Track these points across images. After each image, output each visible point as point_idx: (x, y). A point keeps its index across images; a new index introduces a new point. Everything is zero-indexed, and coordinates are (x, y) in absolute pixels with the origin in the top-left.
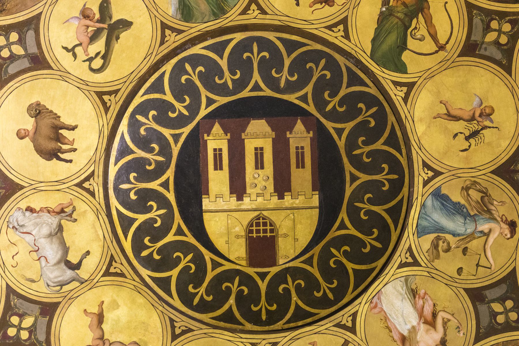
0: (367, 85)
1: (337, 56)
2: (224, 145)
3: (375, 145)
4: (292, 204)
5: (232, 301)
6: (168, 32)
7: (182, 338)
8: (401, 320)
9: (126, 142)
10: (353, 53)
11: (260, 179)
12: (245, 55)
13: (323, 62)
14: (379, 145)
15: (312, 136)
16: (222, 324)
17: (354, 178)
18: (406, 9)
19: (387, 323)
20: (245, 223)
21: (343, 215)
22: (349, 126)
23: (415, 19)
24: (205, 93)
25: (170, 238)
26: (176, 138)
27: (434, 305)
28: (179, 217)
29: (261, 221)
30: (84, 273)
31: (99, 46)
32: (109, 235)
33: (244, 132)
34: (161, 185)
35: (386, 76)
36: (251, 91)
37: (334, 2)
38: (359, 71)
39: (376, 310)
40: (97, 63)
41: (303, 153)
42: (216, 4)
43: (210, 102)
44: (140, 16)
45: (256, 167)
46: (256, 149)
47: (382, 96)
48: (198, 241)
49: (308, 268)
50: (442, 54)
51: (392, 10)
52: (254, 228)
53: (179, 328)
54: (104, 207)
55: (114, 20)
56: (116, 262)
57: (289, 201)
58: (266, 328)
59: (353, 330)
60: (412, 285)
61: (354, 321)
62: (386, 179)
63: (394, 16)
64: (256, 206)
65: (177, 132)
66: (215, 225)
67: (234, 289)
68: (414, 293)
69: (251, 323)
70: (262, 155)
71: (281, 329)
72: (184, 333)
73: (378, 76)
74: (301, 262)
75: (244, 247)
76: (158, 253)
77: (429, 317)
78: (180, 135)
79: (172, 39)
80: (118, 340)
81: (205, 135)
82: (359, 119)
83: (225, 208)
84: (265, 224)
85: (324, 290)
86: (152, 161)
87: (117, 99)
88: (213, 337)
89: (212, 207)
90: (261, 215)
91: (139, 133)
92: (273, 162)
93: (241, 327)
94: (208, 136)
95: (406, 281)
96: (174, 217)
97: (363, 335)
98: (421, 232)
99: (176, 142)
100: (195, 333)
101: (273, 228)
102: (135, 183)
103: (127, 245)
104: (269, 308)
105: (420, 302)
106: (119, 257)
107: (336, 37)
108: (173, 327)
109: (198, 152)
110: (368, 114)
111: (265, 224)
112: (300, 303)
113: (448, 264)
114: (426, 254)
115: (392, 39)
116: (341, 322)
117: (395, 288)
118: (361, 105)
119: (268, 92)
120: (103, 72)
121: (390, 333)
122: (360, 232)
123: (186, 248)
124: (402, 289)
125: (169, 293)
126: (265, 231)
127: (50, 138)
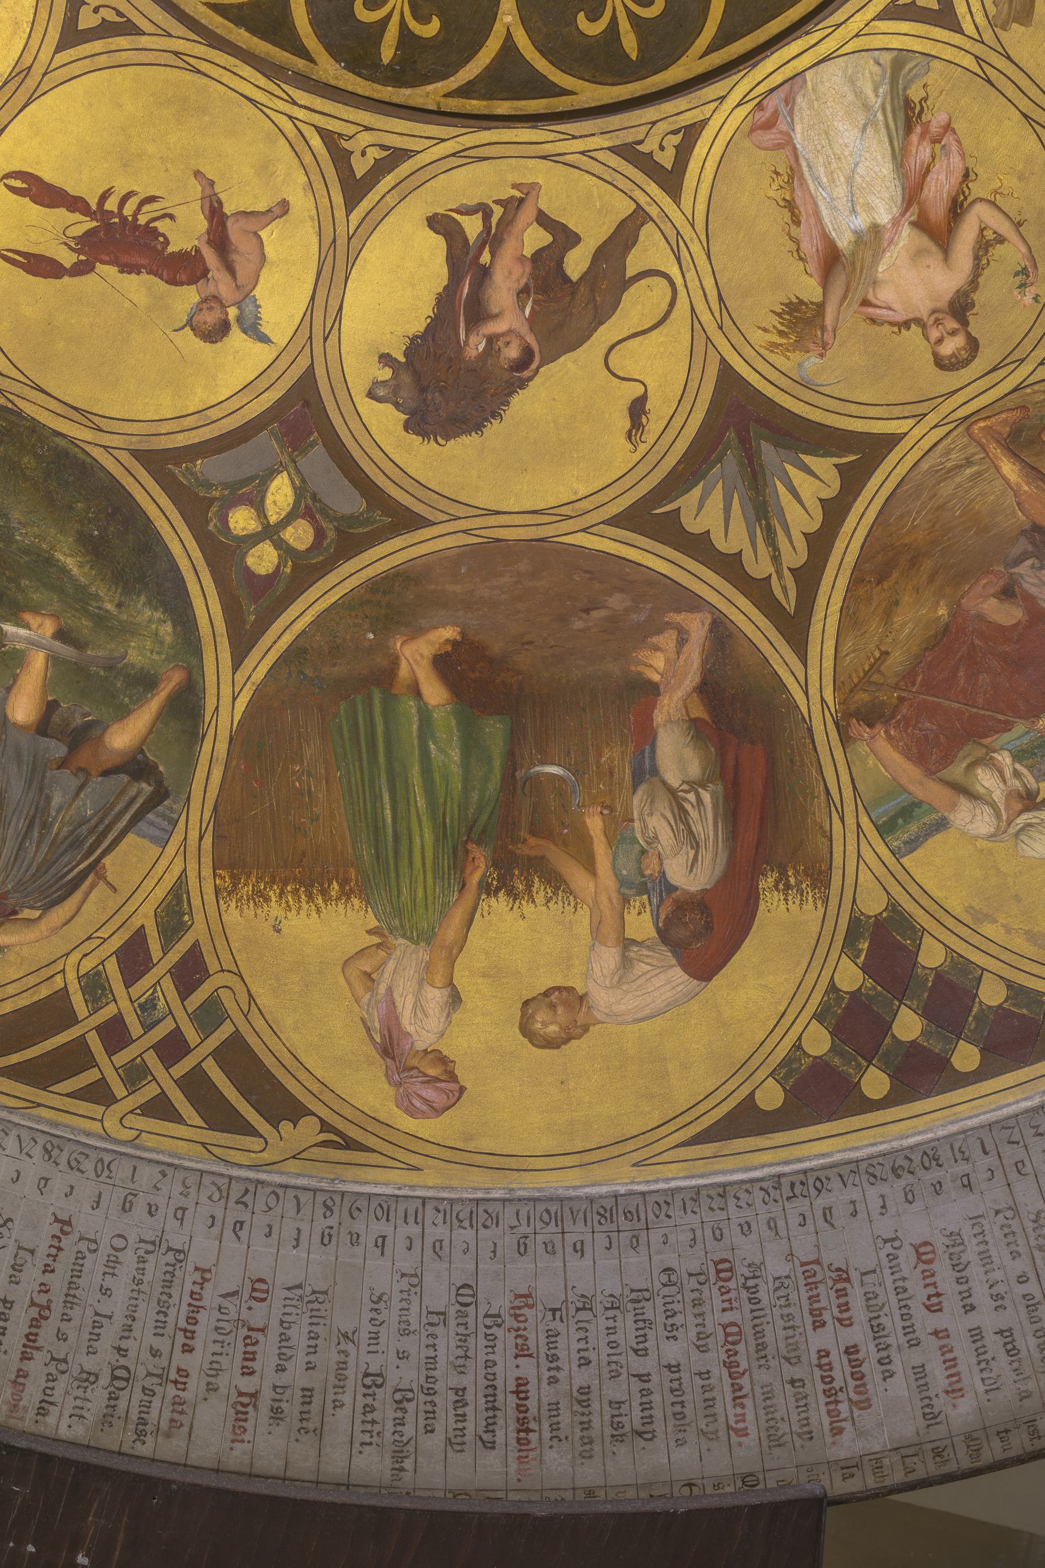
7: (97, 46)
8: (841, 191)
16: (241, 36)
19: (793, 191)
27: (966, 175)
39: (769, 137)
59: (672, 181)
60: (913, 87)
68: (908, 116)
71: (433, 107)
77: (938, 211)
85: (614, 18)
88: (199, 72)
93: (300, 64)
95: (897, 65)
100: (144, 41)
104: (413, 24)
112: (522, 40)
116: (641, 142)
117: (852, 81)
121: (793, 227)
124: (876, 90)
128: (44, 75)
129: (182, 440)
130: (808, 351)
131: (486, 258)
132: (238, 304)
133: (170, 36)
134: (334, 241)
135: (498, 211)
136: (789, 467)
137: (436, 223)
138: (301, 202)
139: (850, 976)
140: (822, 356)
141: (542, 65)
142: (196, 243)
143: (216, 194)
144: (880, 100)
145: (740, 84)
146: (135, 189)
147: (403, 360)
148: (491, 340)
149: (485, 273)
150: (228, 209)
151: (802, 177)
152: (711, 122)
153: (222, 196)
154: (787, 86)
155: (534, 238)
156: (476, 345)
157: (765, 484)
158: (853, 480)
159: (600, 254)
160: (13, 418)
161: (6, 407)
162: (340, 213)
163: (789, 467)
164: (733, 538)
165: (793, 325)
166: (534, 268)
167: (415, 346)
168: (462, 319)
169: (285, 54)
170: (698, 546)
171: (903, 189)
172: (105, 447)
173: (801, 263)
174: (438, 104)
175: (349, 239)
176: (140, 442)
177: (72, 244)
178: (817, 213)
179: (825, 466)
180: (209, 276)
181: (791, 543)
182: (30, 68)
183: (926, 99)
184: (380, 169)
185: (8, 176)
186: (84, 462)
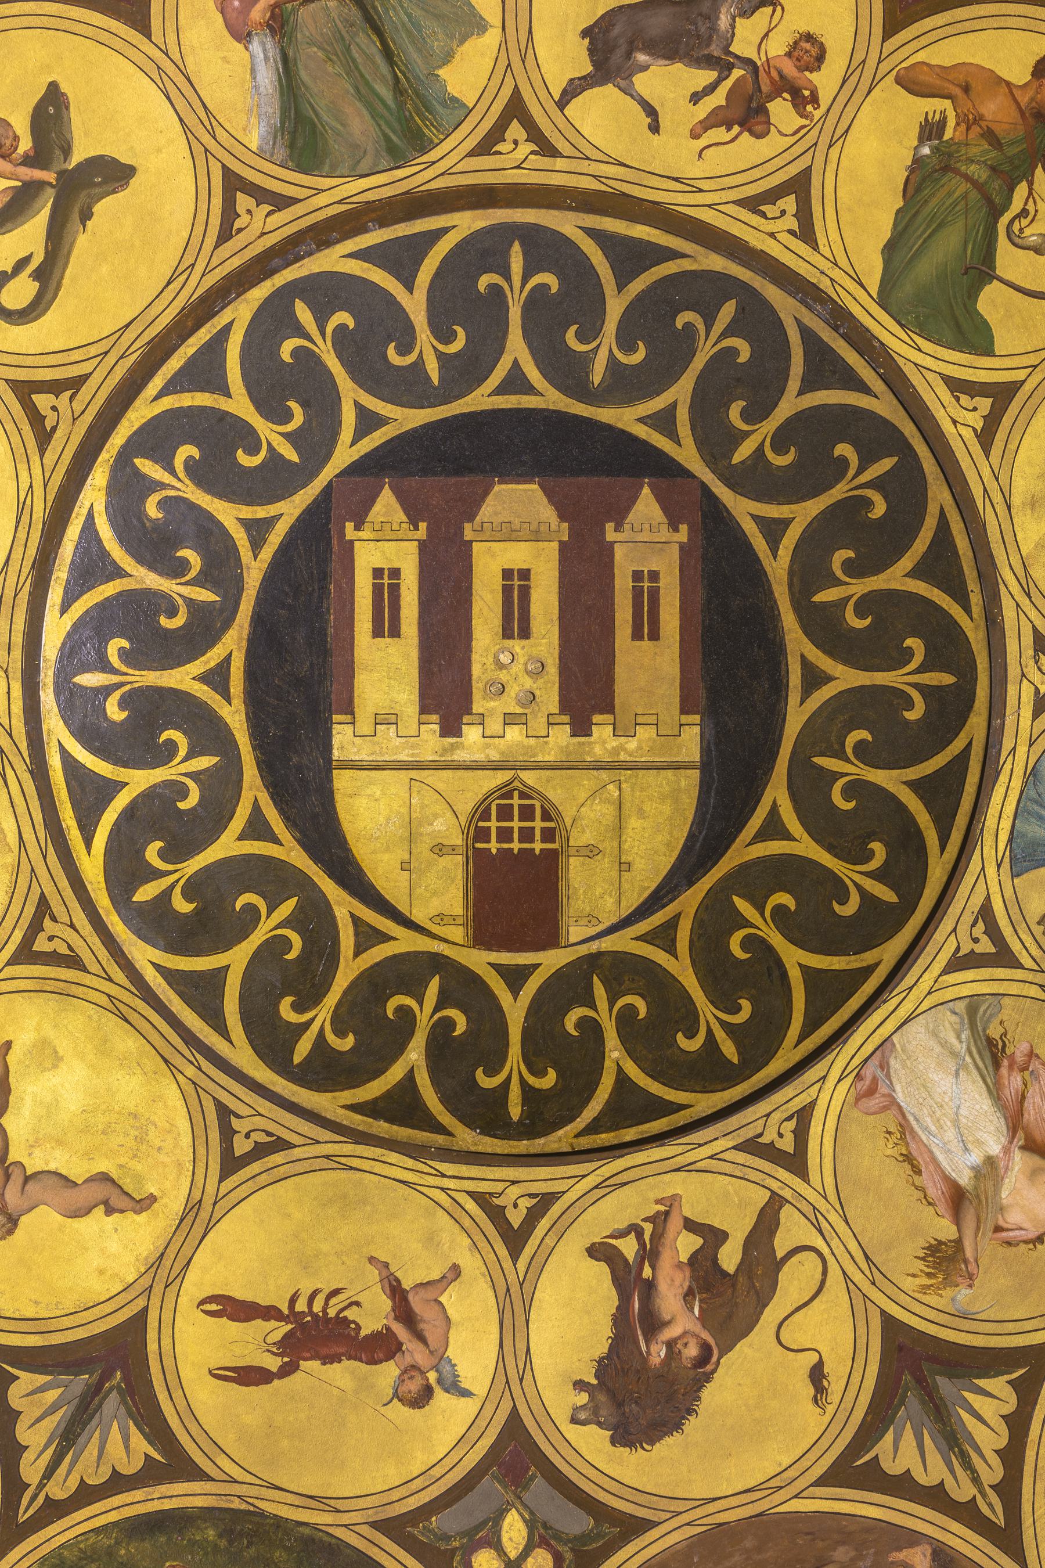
0: (863, 388)
1: (772, 293)
2: (405, 557)
3: (882, 576)
4: (616, 751)
5: (415, 1054)
6: (244, 202)
8: (951, 1134)
9: (99, 541)
10: (825, 284)
11: (517, 668)
12: (484, 282)
13: (728, 311)
14: (897, 577)
15: (686, 540)
16: (382, 1128)
17: (814, 679)
18: (994, 154)
19: (907, 1145)
20: (465, 806)
21: (777, 793)
22: (804, 513)
23: (1024, 184)
24: (352, 394)
25: (227, 845)
26: (257, 530)
28: (259, 781)
29: (516, 801)
31: (29, 237)
32: (36, 835)
33: (471, 518)
34: (204, 678)
35: (927, 362)
36: (499, 391)
37: (769, 123)
38: (842, 343)
39: (874, 1102)
40: (20, 292)
41: (654, 594)
42: (399, 121)
43: (368, 422)
44: (159, 150)
45: (504, 629)
46: (507, 574)
47: (912, 424)
48: (316, 858)
49: (661, 957)
51: (950, 155)
52: (493, 824)
53: (247, 1136)
54: (24, 746)
55: (77, 158)
56: (54, 919)
57: (604, 742)
58: (523, 1146)
59: (796, 1162)
60: (991, 1027)
61: (801, 1135)
62: (915, 686)
63: (957, 172)
64: (502, 754)
65: (261, 512)
66: (370, 810)
67: (424, 1017)
68: (993, 1054)
69: (474, 1129)
70: (525, 593)
71: (566, 1149)
72: (260, 1151)
73: (900, 361)
74: (637, 939)
75: (460, 882)
76: (187, 896)
78: (269, 523)
79: (257, 226)
80: (52, 1166)
81: (349, 526)
82: (838, 492)
83: (403, 756)
84: (527, 813)
85: (710, 1031)
86: (180, 601)
87: (78, 406)
88: (352, 1168)
89: (362, 753)
90: (516, 784)
91: (141, 514)
92: (561, 617)
93: (440, 1139)
94: (358, 528)
96: (240, 781)
97: (829, 1180)
98: (1024, 857)
99: (256, 545)
100: (297, 1153)
101: (552, 825)
102: (124, 668)
103: (92, 866)
104: (531, 1080)
105: (1014, 1082)
106: (65, 903)
107: (772, 235)
108: (227, 1133)
109: (325, 578)
110: (864, 478)
111: (527, 813)
112: (632, 1070)
114: (1038, 930)
115: (948, 245)
116: (760, 1135)
117: (935, 1034)
118: (843, 449)
119: (550, 398)
120: (36, 319)
122: (830, 849)
123: (273, 879)
124: (958, 1037)
125: (217, 1022)
126: (527, 835)
128: (215, 1204)
129: (413, 1503)
130: (957, 1285)
131: (647, 1272)
132: (436, 1368)
133: (318, 1142)
134: (508, 1290)
135: (648, 1228)
136: (966, 1394)
137: (595, 1252)
138: (470, 1263)
140: (970, 1286)
141: (655, 1088)
142: (385, 1321)
143: (392, 1274)
144: (964, 1046)
145: (836, 1061)
146: (319, 1286)
147: (595, 1382)
148: (670, 1344)
149: (650, 1286)
150: (407, 1285)
151: (912, 1131)
152: (818, 1102)
153: (398, 1274)
154: (878, 1053)
155: (687, 1244)
156: (658, 1353)
157: (950, 1415)
159: (749, 1243)
160: (257, 1519)
161: (249, 1511)
162: (507, 1264)
163: (966, 1394)
164: (932, 1469)
165: (937, 1265)
166: (693, 1271)
167: (603, 1367)
168: (639, 1332)
169: (424, 1134)
170: (903, 1486)
171: (1006, 1119)
172: (345, 1526)
173: (931, 1207)
174: (572, 1145)
175: (521, 1285)
176: (377, 1513)
177: (275, 1350)
178: (934, 1160)
179: (998, 1385)
180: (404, 1348)
181: (986, 1462)
182: (200, 1201)
183: (1005, 1034)
184: (533, 1216)
185: (202, 1302)
186: (330, 1544)
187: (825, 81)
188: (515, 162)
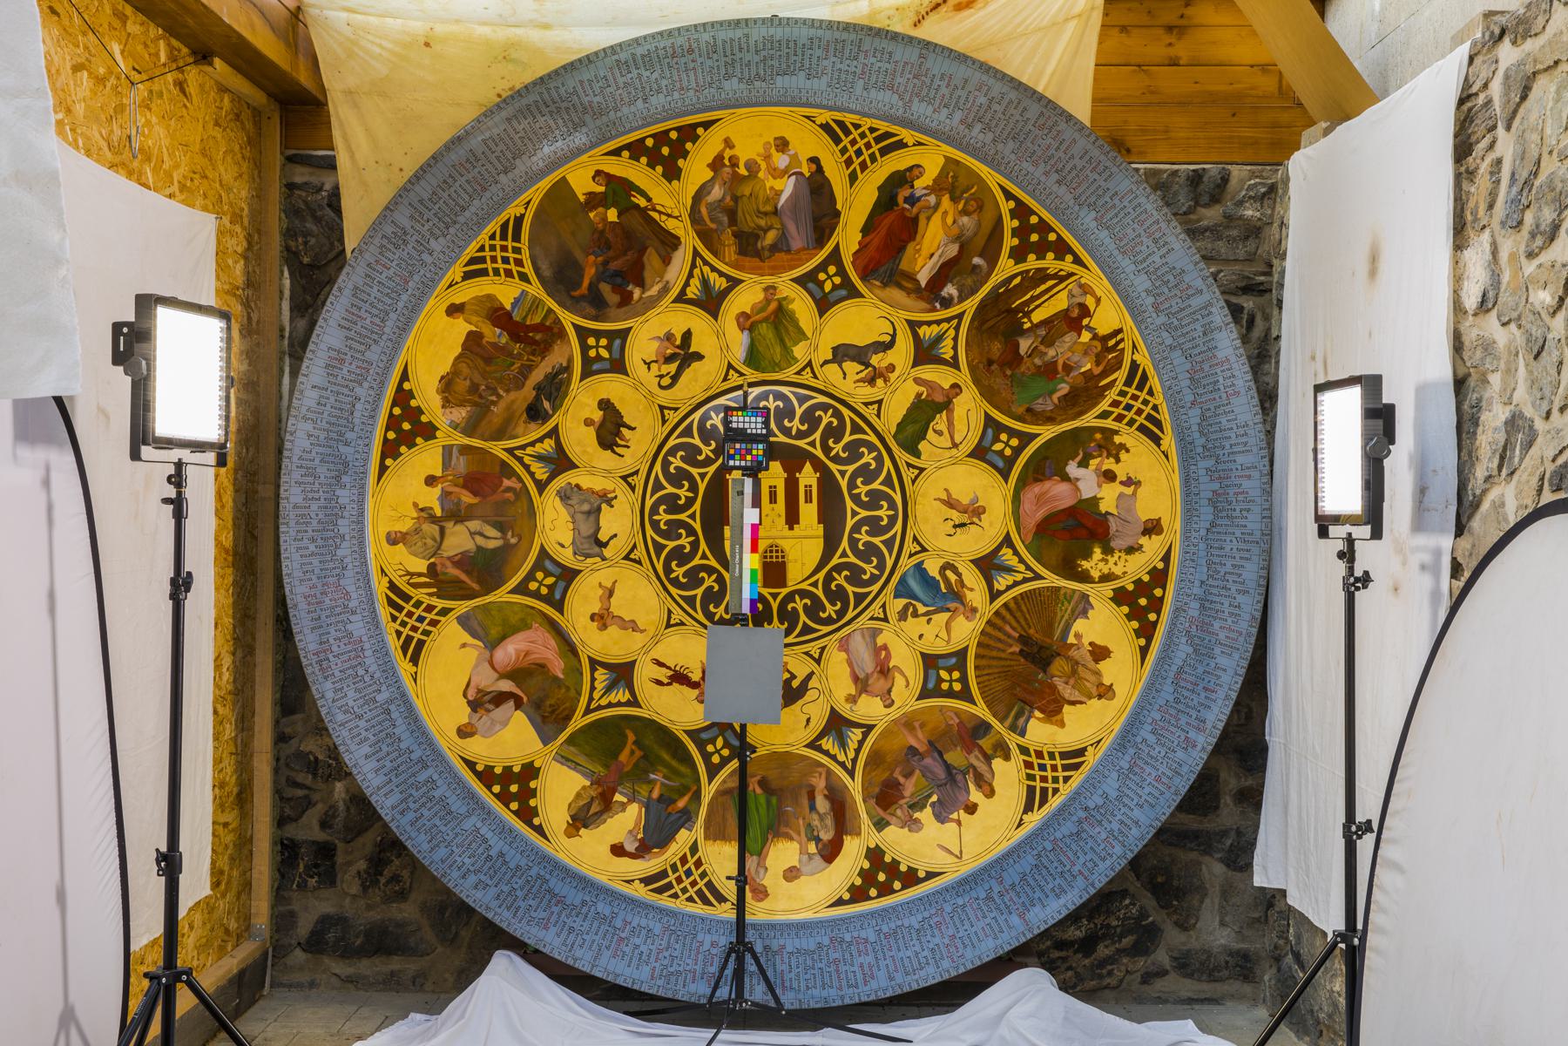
30: (607, 552)
31: (673, 368)
35: (903, 457)
40: (666, 381)
50: (954, 451)
59: (818, 661)
106: (641, 546)
113: (913, 626)
127: (611, 430)
139: (867, 865)
158: (865, 735)
170: (826, 753)
187: (893, 376)
188: (806, 377)
